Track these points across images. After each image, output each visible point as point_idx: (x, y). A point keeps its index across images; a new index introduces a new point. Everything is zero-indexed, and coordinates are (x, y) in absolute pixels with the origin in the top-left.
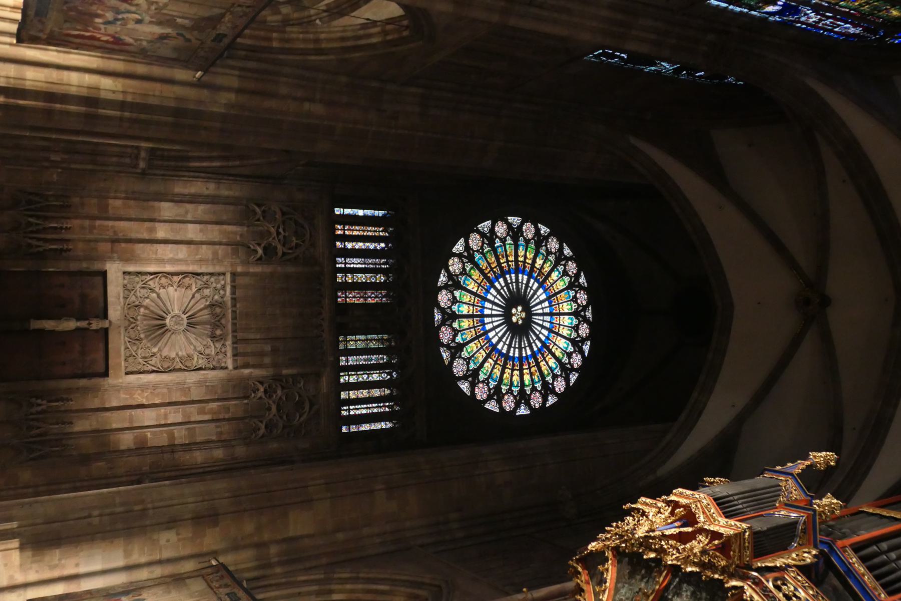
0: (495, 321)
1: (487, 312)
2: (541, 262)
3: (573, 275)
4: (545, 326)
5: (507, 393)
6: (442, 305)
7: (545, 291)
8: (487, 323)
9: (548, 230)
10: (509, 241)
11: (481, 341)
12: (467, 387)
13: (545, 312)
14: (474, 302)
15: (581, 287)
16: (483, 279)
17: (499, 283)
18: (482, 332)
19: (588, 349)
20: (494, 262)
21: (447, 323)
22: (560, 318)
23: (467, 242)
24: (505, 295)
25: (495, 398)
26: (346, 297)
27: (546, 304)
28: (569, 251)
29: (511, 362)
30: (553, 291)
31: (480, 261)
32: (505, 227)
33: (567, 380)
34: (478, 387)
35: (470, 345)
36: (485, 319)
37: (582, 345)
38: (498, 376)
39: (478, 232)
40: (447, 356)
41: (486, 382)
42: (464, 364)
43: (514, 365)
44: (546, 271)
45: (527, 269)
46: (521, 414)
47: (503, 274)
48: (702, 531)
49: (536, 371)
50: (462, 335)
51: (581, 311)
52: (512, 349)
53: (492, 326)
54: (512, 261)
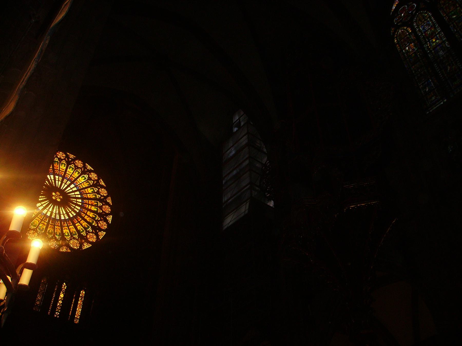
4: (69, 184)
12: (86, 245)
14: (40, 219)
18: (59, 222)
19: (90, 167)
22: (67, 173)
25: (98, 231)
27: (57, 177)
36: (52, 217)
37: (87, 169)
42: (73, 241)
43: (84, 213)
46: (111, 221)
50: (57, 235)
51: (68, 160)
52: (75, 209)
53: (58, 215)
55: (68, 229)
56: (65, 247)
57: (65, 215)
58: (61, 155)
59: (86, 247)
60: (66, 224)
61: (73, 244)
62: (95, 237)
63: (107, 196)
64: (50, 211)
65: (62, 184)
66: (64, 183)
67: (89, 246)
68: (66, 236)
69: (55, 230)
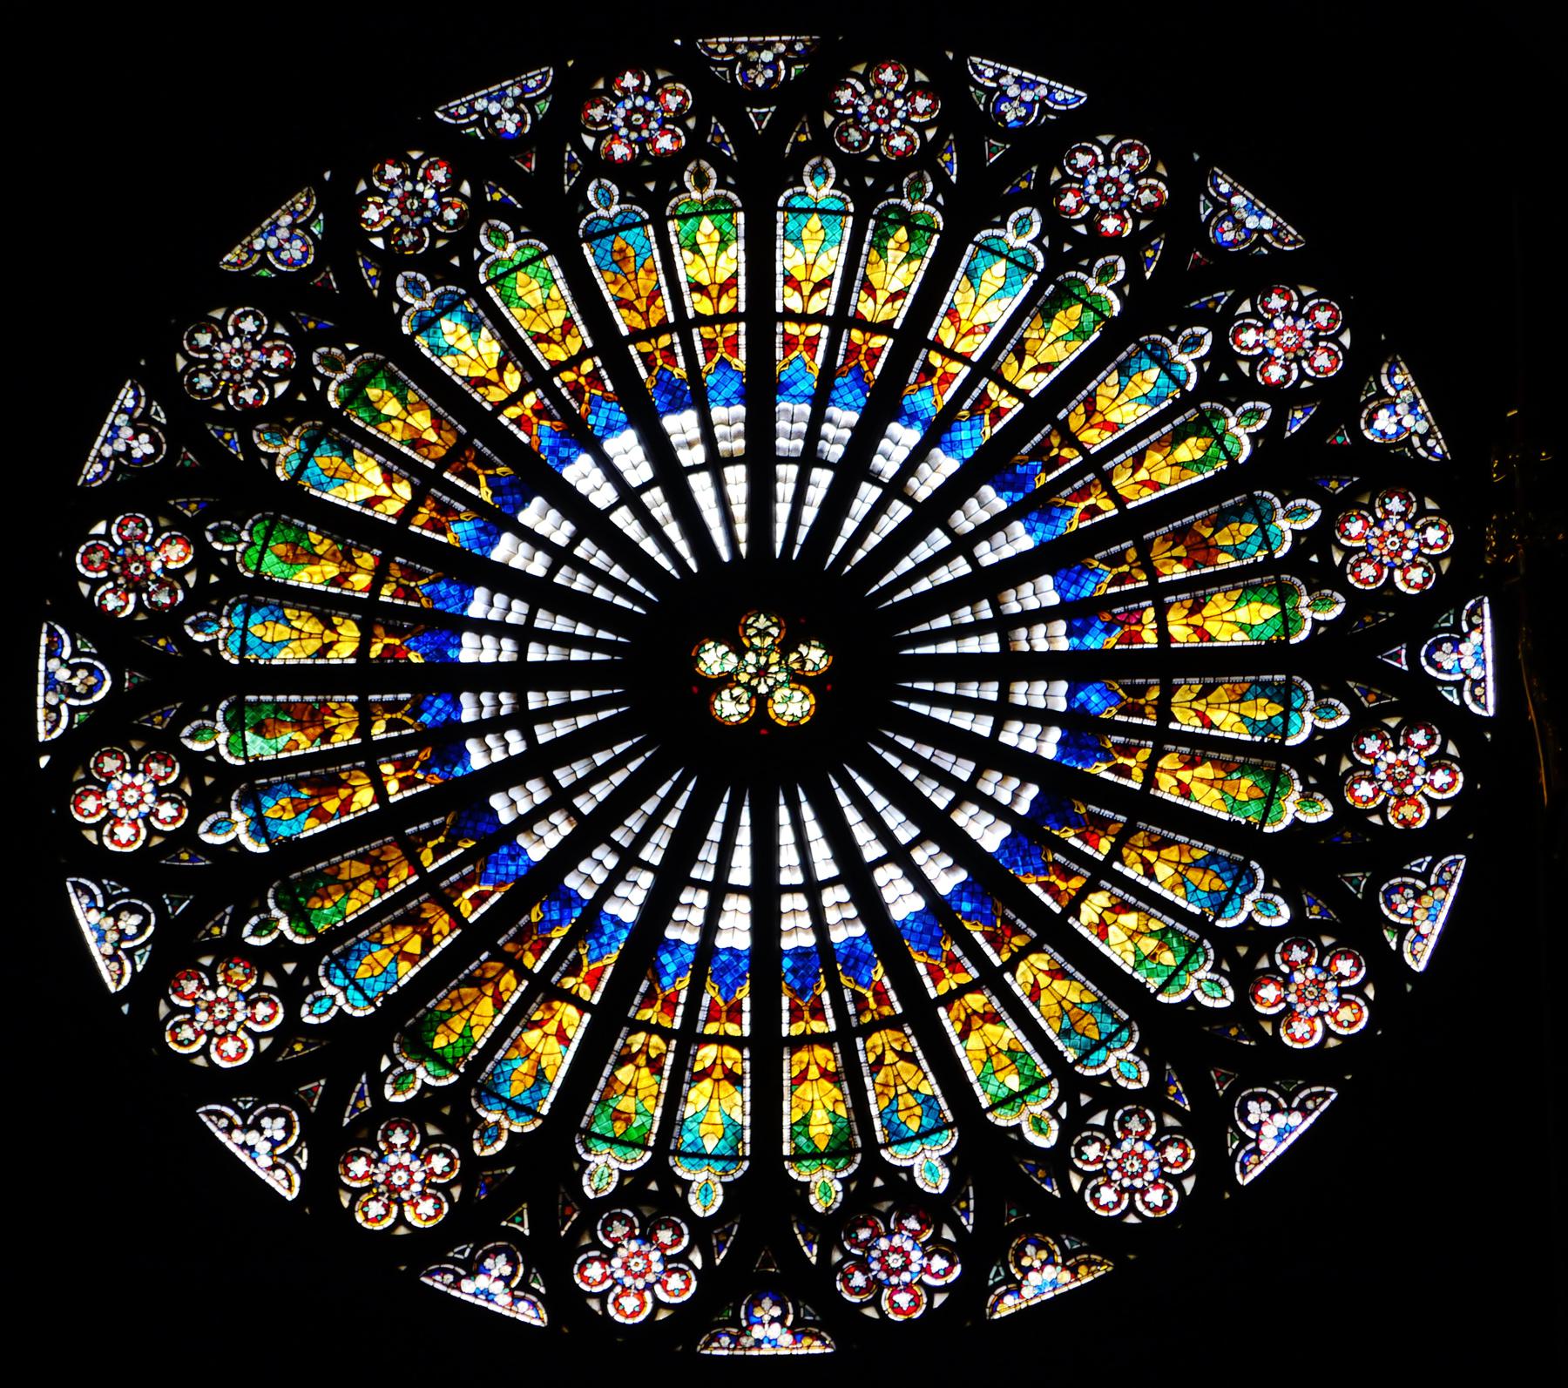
0: (806, 865)
1: (736, 930)
3: (466, 188)
4: (851, 447)
6: (678, 1289)
8: (820, 926)
9: (127, 397)
11: (951, 982)
13: (739, 445)
14: (666, 1034)
17: (525, 823)
18: (879, 973)
21: (812, 1255)
22: (789, 315)
24: (618, 778)
27: (681, 426)
30: (587, 366)
31: (362, 972)
32: (110, 764)
34: (1276, 1020)
35: (972, 1077)
36: (787, 943)
49: (1178, 537)
50: (897, 1138)
51: (740, 128)
52: (1011, 735)
53: (841, 893)
55: (1004, 1015)
56: (1040, 1246)
57: (919, 856)
58: (638, 118)
59: (1280, 1137)
60: (966, 963)
61: (1120, 1168)
64: (739, 890)
65: (773, 479)
66: (787, 460)
67: (1306, 1113)
68: (1011, 1099)
69: (868, 1081)
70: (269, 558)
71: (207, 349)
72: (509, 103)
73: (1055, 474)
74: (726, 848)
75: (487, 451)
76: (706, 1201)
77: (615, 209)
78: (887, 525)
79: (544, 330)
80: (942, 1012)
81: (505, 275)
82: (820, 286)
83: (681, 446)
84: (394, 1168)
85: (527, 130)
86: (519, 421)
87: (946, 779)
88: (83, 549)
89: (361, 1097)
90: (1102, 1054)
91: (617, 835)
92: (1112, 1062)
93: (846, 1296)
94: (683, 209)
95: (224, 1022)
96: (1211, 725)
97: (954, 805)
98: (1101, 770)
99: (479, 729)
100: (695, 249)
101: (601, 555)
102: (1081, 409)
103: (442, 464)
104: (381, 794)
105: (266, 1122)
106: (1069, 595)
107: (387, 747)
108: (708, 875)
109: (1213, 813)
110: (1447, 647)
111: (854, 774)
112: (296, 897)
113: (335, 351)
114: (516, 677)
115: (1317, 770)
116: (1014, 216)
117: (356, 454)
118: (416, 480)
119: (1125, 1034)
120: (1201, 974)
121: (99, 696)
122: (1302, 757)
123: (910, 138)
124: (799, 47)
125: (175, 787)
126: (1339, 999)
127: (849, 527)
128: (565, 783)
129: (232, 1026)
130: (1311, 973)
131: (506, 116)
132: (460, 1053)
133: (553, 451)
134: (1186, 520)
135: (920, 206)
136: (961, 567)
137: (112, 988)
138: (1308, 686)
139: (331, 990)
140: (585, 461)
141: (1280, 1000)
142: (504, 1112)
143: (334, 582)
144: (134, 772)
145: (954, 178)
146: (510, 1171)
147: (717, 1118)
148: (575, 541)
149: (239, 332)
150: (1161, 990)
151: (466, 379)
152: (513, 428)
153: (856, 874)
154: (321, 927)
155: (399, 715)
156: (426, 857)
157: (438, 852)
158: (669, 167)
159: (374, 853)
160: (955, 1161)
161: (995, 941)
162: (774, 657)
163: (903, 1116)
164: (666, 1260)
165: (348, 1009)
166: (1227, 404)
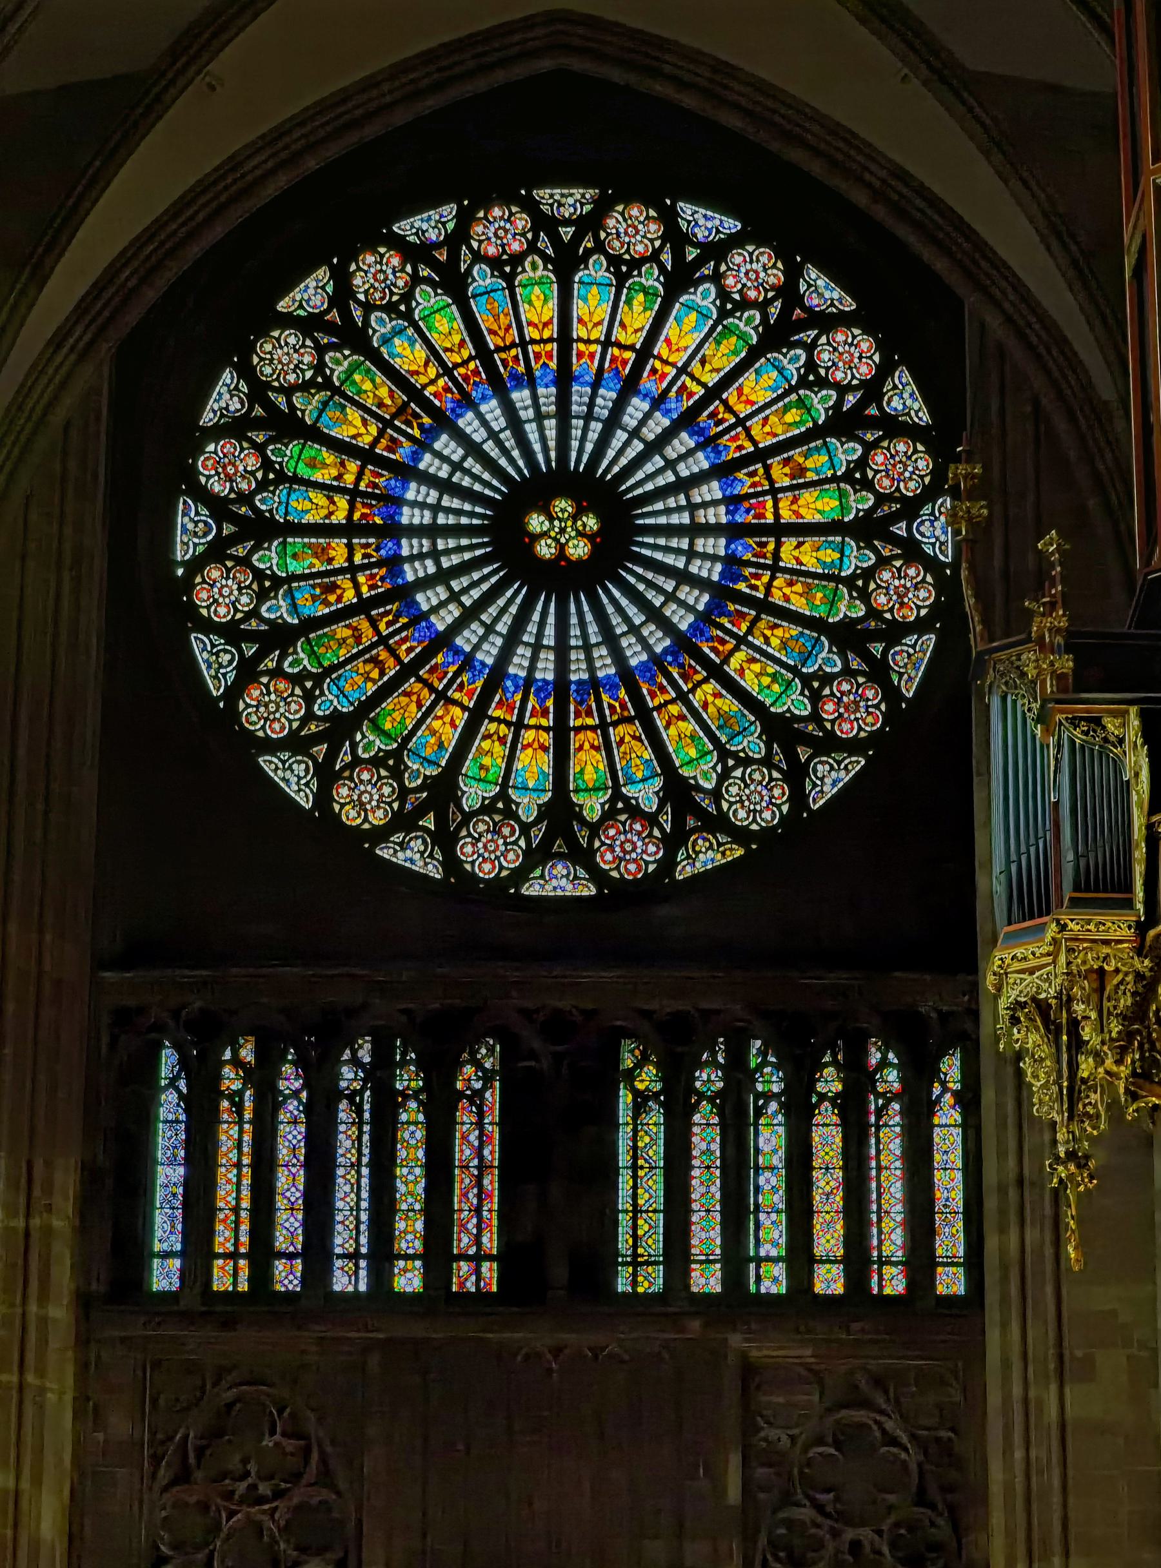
0: (585, 635)
1: (546, 671)
2: (354, 415)
3: (409, 268)
4: (611, 411)
5: (865, 596)
6: (512, 860)
7: (467, 402)
8: (591, 669)
9: (227, 376)
10: (268, 559)
11: (660, 699)
13: (553, 408)
15: (459, 237)
16: (420, 679)
17: (434, 610)
18: (622, 694)
19: (709, 213)
20: (355, 629)
22: (580, 340)
23: (270, 746)
26: (478, 1259)
27: (521, 397)
28: (311, 282)
29: (748, 571)
31: (348, 688)
32: (215, 574)
33: (826, 322)
34: (833, 722)
35: (671, 750)
36: (574, 677)
38: (795, 631)
39: (234, 693)
40: (711, 847)
41: (816, 684)
44: (391, 394)
45: (381, 481)
47: (403, 593)
48: (1065, 1000)
49: (786, 462)
51: (555, 239)
53: (604, 651)
54: (350, 547)
57: (645, 632)
58: (501, 233)
59: (834, 784)
60: (669, 688)
61: (748, 799)
62: (870, 694)
63: (884, 371)
64: (548, 647)
66: (578, 417)
70: (301, 465)
71: (270, 353)
72: (433, 224)
73: (720, 428)
74: (542, 624)
75: (418, 410)
76: (528, 814)
77: (488, 281)
78: (631, 453)
79: (449, 346)
80: (655, 714)
81: (429, 316)
82: (596, 325)
83: (521, 409)
84: (362, 793)
85: (442, 238)
86: (436, 395)
87: (660, 590)
88: (202, 458)
89: (346, 753)
90: (741, 737)
91: (484, 617)
92: (745, 743)
93: (602, 865)
94: (524, 282)
95: (274, 713)
96: (801, 564)
97: (663, 604)
98: (742, 586)
99: (412, 558)
100: (530, 303)
101: (478, 466)
102: (735, 393)
103: (394, 416)
104: (358, 593)
105: (295, 766)
106: (727, 493)
107: (363, 568)
108: (532, 641)
109: (801, 611)
110: (927, 524)
111: (610, 586)
112: (312, 647)
113: (338, 355)
114: (432, 531)
115: (857, 588)
116: (701, 289)
117: (348, 410)
118: (380, 426)
119: (753, 728)
120: (793, 697)
121: (210, 538)
122: (849, 582)
123: (646, 246)
124: (588, 196)
125: (249, 587)
126: (867, 711)
127: (611, 454)
128: (457, 589)
129: (277, 715)
130: (852, 697)
131: (431, 230)
132: (398, 732)
133: (453, 410)
134: (791, 453)
135: (650, 282)
136: (670, 477)
137: (215, 693)
138: (853, 543)
139: (331, 697)
140: (470, 415)
141: (835, 711)
142: (422, 764)
143: (336, 478)
144: (227, 578)
145: (669, 268)
146: (425, 795)
147: (535, 770)
148: (464, 459)
149: (287, 344)
150: (772, 705)
151: (408, 371)
152: (432, 398)
153: (610, 639)
154: (326, 663)
155: (369, 551)
156: (382, 626)
157: (389, 624)
158: (517, 260)
159: (354, 624)
160: (661, 794)
161: (686, 677)
162: (569, 523)
163: (634, 770)
164: (506, 844)
165: (339, 708)
166: (813, 391)
